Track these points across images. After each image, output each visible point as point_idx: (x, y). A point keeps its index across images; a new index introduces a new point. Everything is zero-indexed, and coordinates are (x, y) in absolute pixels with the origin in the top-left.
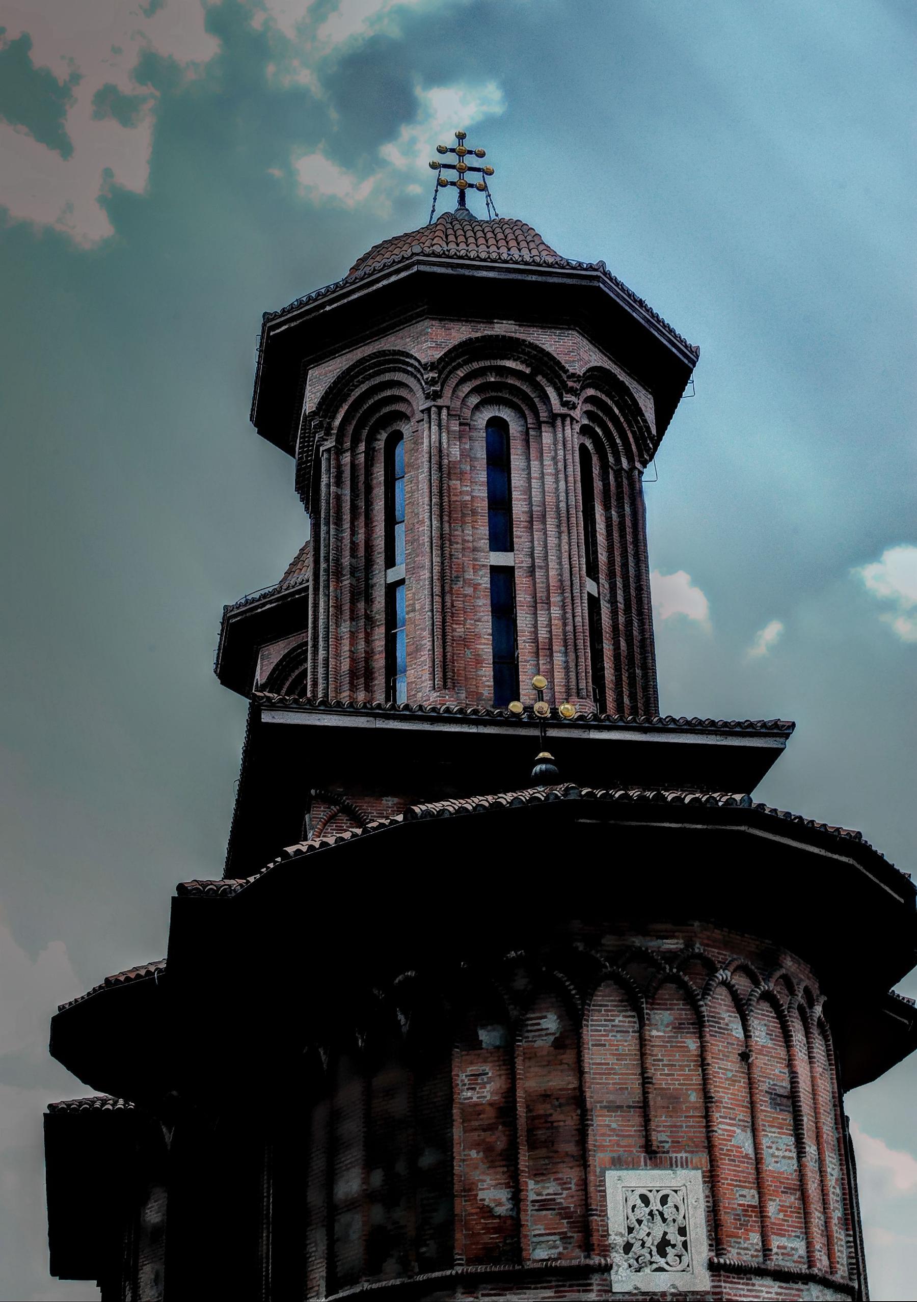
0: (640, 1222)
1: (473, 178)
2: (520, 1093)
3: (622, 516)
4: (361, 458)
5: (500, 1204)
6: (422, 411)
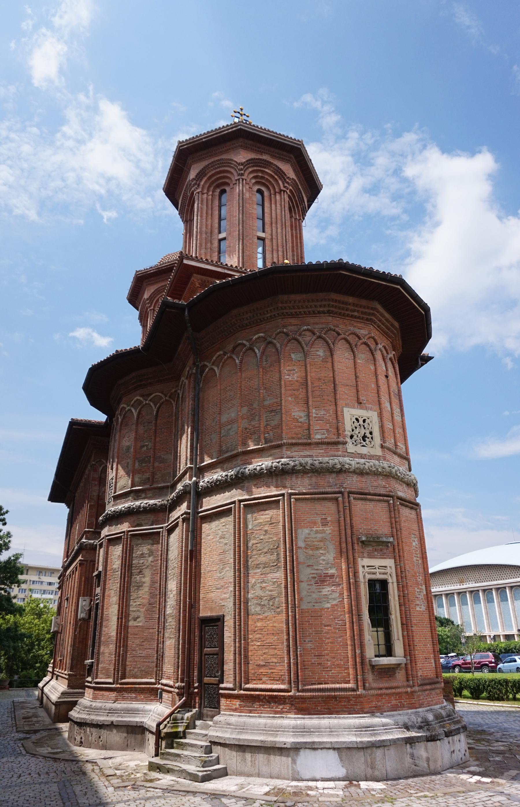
0: (356, 428)
2: (309, 377)
3: (296, 233)
4: (210, 197)
5: (301, 417)
6: (236, 180)
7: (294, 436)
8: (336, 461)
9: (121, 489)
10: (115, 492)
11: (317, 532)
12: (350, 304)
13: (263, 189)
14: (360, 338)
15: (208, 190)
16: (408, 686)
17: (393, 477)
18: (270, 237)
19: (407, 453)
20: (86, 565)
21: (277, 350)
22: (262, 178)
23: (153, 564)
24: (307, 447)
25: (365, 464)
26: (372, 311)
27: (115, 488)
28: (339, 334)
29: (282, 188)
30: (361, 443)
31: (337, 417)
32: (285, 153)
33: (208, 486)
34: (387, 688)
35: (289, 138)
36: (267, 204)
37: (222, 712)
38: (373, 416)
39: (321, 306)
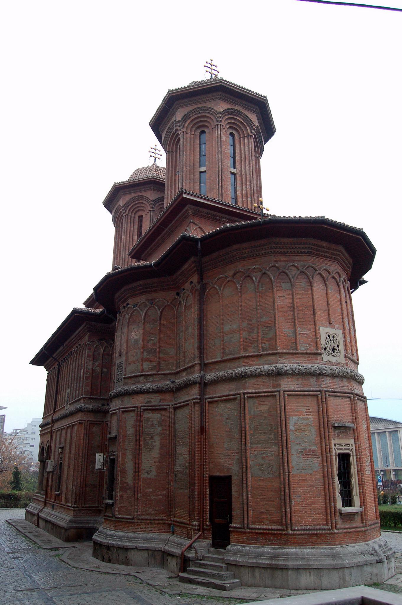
0: (328, 342)
1: (214, 72)
5: (290, 333)
6: (215, 125)
7: (285, 347)
8: (317, 368)
9: (132, 373)
10: (125, 375)
11: (303, 419)
12: (323, 247)
13: (234, 132)
14: (329, 273)
15: (191, 131)
16: (364, 527)
17: (353, 379)
18: (239, 173)
19: (358, 360)
20: (85, 424)
21: (271, 280)
22: (234, 124)
23: (161, 432)
24: (295, 356)
25: (335, 370)
26: (338, 253)
27: (126, 371)
28: (316, 270)
29: (250, 133)
30: (331, 354)
31: (316, 334)
32: (253, 105)
33: (214, 379)
34: (350, 528)
35: (257, 95)
36: (237, 145)
37: (231, 543)
38: (339, 332)
39: (303, 248)
